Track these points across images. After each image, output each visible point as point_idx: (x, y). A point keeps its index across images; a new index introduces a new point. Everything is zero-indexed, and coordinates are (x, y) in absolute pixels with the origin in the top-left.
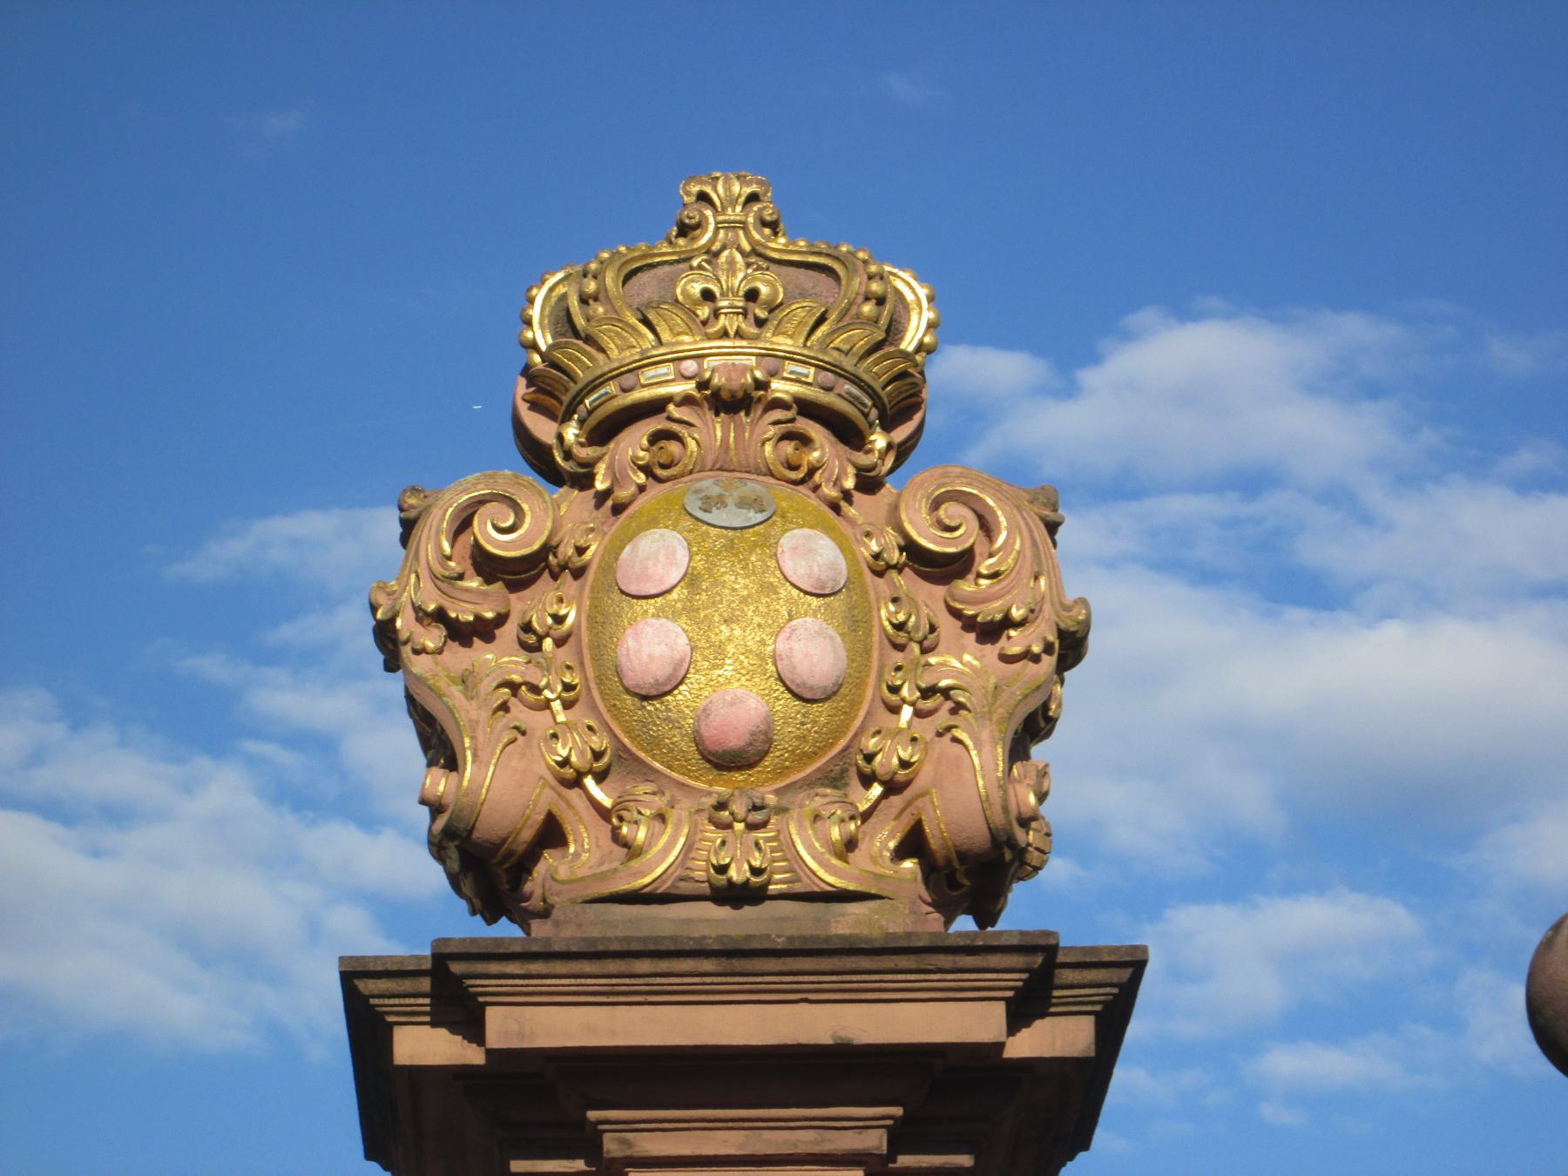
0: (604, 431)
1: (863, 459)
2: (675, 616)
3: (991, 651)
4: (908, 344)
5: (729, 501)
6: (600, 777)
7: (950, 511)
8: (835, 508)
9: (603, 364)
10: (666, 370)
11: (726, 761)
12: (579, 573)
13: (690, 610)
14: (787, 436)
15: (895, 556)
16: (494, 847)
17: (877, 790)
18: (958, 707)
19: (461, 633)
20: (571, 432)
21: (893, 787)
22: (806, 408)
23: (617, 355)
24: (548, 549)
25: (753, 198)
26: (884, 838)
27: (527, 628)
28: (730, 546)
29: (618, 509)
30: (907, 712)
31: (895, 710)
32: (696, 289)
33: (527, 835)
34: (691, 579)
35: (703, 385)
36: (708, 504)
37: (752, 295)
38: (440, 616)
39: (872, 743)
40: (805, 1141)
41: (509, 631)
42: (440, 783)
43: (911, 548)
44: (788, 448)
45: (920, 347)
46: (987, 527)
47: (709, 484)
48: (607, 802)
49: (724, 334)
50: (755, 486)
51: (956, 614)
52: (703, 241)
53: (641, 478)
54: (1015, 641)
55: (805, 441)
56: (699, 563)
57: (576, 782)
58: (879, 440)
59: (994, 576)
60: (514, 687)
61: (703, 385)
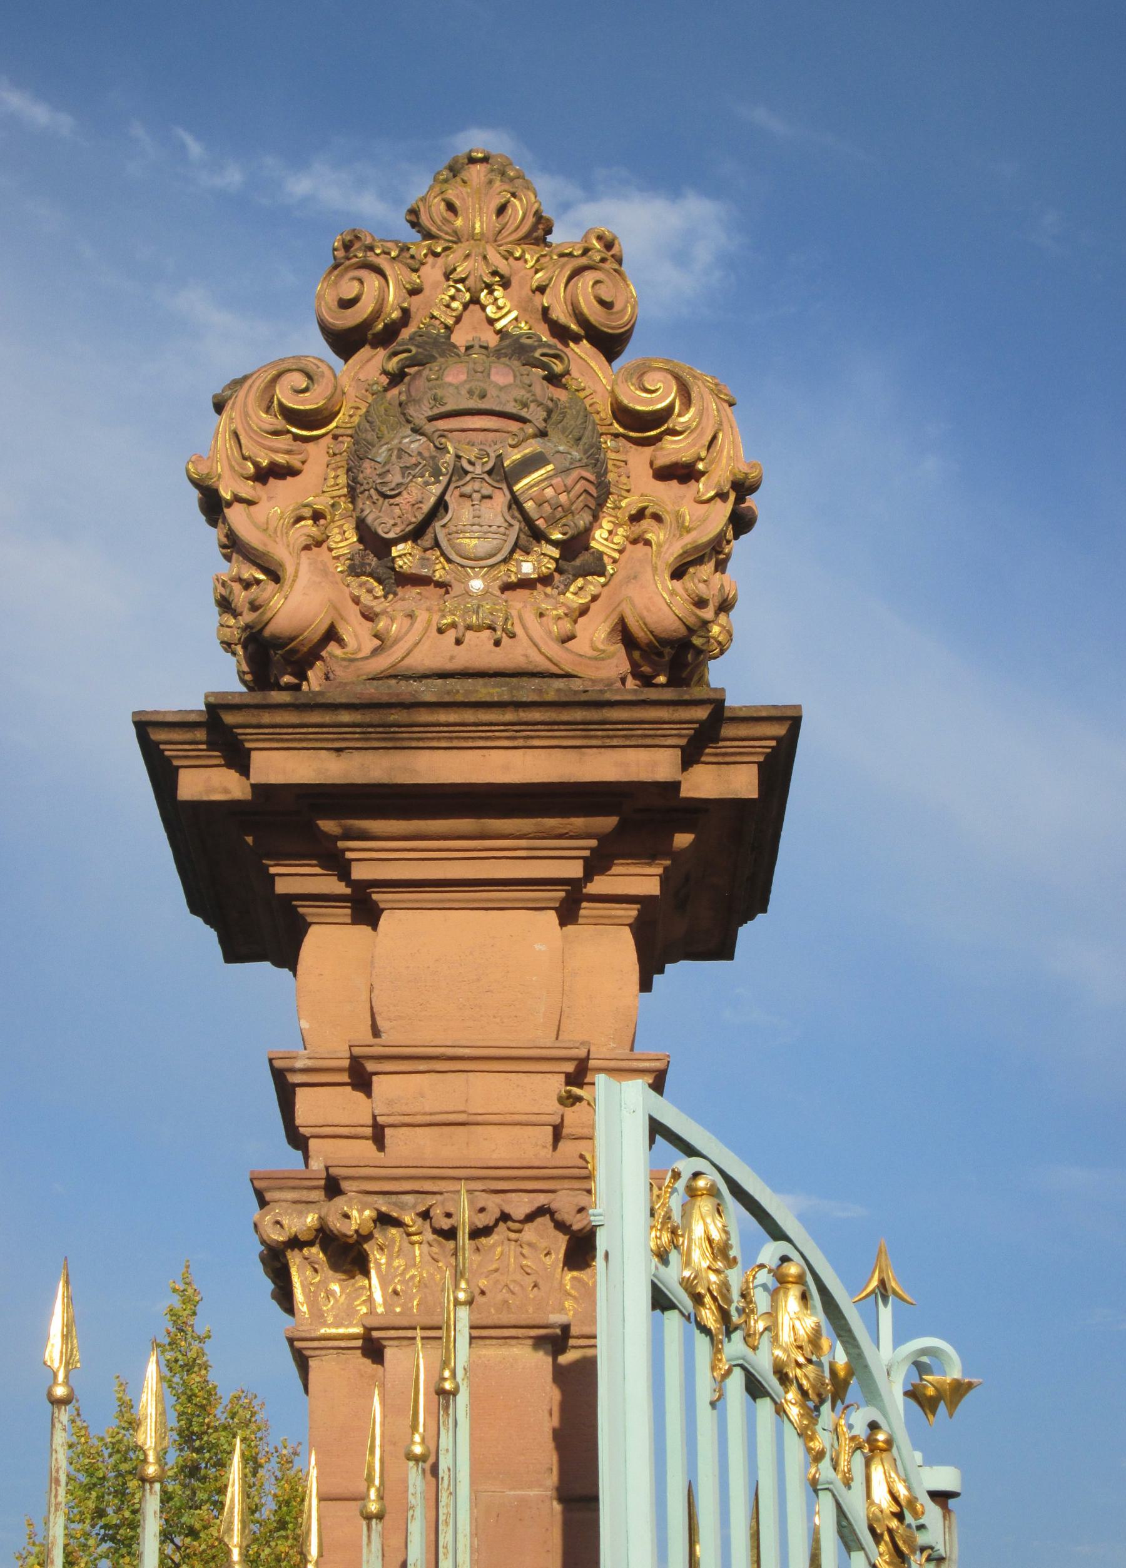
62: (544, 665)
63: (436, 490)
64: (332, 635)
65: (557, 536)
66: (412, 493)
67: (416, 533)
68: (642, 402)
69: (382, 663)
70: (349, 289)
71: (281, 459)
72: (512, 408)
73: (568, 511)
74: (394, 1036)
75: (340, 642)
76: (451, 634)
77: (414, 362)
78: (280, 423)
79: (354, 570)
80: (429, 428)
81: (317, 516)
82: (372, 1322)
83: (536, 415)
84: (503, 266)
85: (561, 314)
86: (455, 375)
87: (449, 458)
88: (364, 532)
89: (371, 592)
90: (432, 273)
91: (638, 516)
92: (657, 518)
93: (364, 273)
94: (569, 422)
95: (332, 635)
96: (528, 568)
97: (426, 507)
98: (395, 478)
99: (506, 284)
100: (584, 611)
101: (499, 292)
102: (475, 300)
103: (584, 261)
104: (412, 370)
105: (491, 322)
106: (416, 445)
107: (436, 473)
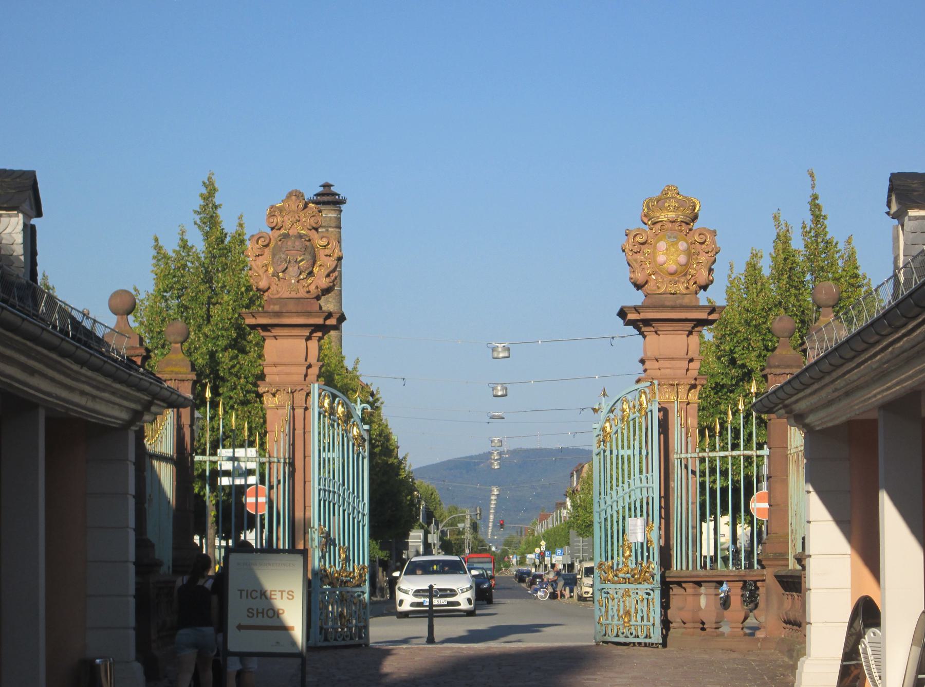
4: (696, 211)
7: (702, 236)
10: (663, 217)
11: (671, 274)
13: (667, 254)
22: (682, 221)
34: (667, 249)
40: (681, 328)
62: (303, 296)
69: (277, 296)
70: (272, 220)
72: (299, 249)
91: (321, 265)
96: (301, 277)
106: (283, 256)
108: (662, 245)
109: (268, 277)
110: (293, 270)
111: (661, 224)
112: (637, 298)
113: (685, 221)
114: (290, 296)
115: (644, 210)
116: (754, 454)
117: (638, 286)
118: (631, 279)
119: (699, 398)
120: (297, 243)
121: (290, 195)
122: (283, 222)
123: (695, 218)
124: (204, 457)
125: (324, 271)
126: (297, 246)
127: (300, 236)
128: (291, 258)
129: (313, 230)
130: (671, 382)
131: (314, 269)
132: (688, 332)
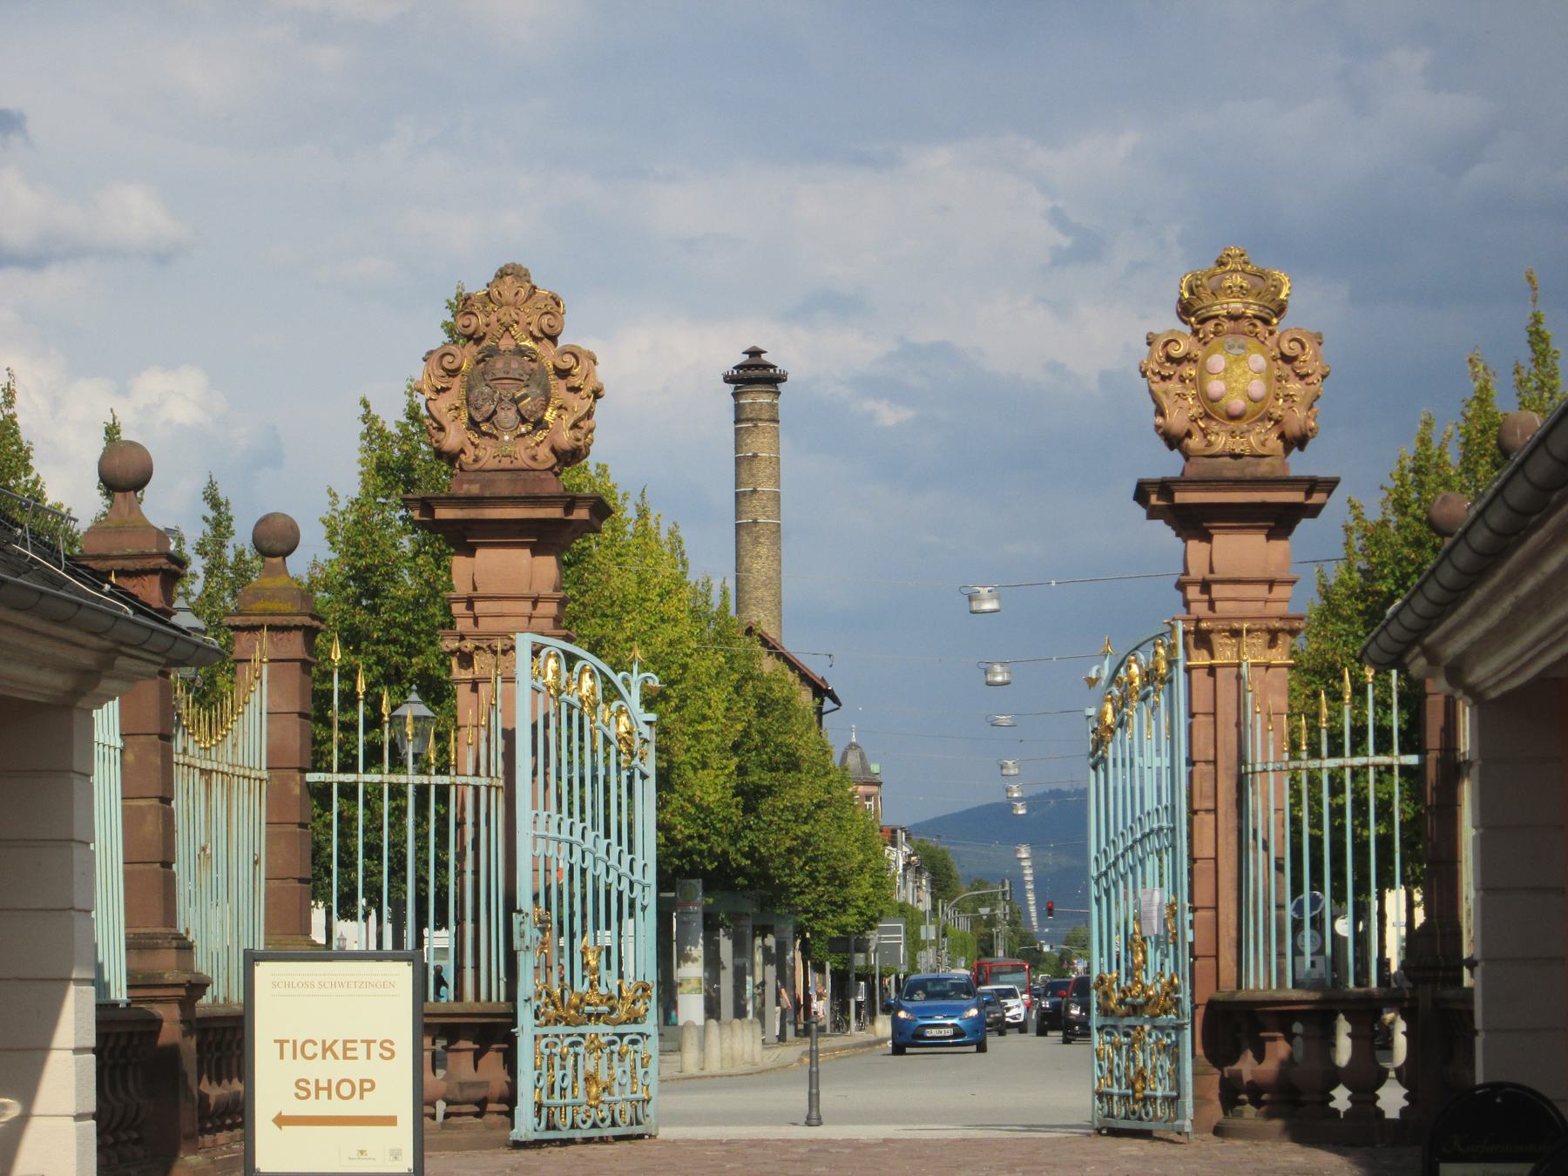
0: (1203, 321)
1: (1270, 328)
2: (1221, 379)
3: (1303, 382)
4: (1282, 296)
5: (1236, 345)
6: (1201, 419)
7: (1295, 345)
8: (1263, 342)
9: (1202, 305)
11: (1233, 418)
12: (1195, 361)
13: (1225, 378)
14: (1251, 324)
15: (1279, 356)
16: (1175, 436)
17: (1272, 423)
18: (1294, 401)
19: (1164, 378)
20: (1193, 319)
21: (1277, 422)
22: (1256, 317)
23: (1206, 303)
24: (1188, 354)
25: (1242, 255)
26: (1274, 435)
27: (1181, 376)
28: (1236, 360)
29: (1205, 344)
30: (1281, 401)
31: (1277, 399)
32: (1227, 285)
33: (1183, 435)
34: (1226, 370)
35: (1228, 313)
36: (1231, 347)
37: (1242, 287)
38: (1159, 373)
39: (1272, 410)
41: (1176, 378)
42: (1160, 420)
43: (1282, 353)
44: (1251, 328)
45: (1287, 295)
46: (1303, 347)
47: (1230, 339)
48: (1203, 426)
49: (1234, 297)
50: (1242, 340)
51: (1294, 371)
52: (1228, 268)
53: (1212, 336)
54: (1310, 380)
55: (1255, 326)
56: (1228, 365)
57: (1195, 421)
58: (1275, 321)
59: (1304, 361)
60: (1178, 395)
61: (1228, 313)
62: (525, 466)
63: (493, 407)
64: (462, 451)
65: (532, 420)
66: (484, 409)
67: (488, 419)
68: (562, 365)
69: (476, 466)
71: (444, 386)
72: (517, 377)
73: (536, 412)
74: (481, 591)
75: (465, 453)
76: (497, 459)
77: (487, 356)
78: (444, 374)
79: (468, 429)
80: (492, 384)
81: (457, 408)
82: (474, 676)
83: (525, 377)
84: (516, 318)
85: (537, 334)
86: (499, 365)
87: (497, 395)
88: (471, 419)
89: (474, 437)
90: (493, 318)
91: (560, 407)
92: (566, 409)
93: (471, 316)
94: (538, 377)
95: (462, 451)
97: (490, 413)
98: (480, 402)
99: (517, 323)
100: (542, 442)
101: (515, 326)
102: (507, 330)
103: (545, 310)
104: (487, 359)
105: (513, 337)
106: (487, 390)
107: (493, 401)
108: (1217, 361)
109: (459, 430)
110: (508, 416)
111: (1215, 321)
112: (1169, 465)
113: (1262, 314)
114: (501, 466)
115: (1182, 295)
116: (1396, 762)
117: (1173, 441)
118: (1158, 427)
119: (1290, 658)
120: (514, 365)
121: (502, 274)
122: (488, 325)
123: (1280, 310)
124: (328, 775)
125: (568, 419)
126: (515, 370)
127: (520, 352)
128: (504, 392)
129: (546, 341)
130: (1236, 625)
131: (548, 414)
132: (1266, 531)
